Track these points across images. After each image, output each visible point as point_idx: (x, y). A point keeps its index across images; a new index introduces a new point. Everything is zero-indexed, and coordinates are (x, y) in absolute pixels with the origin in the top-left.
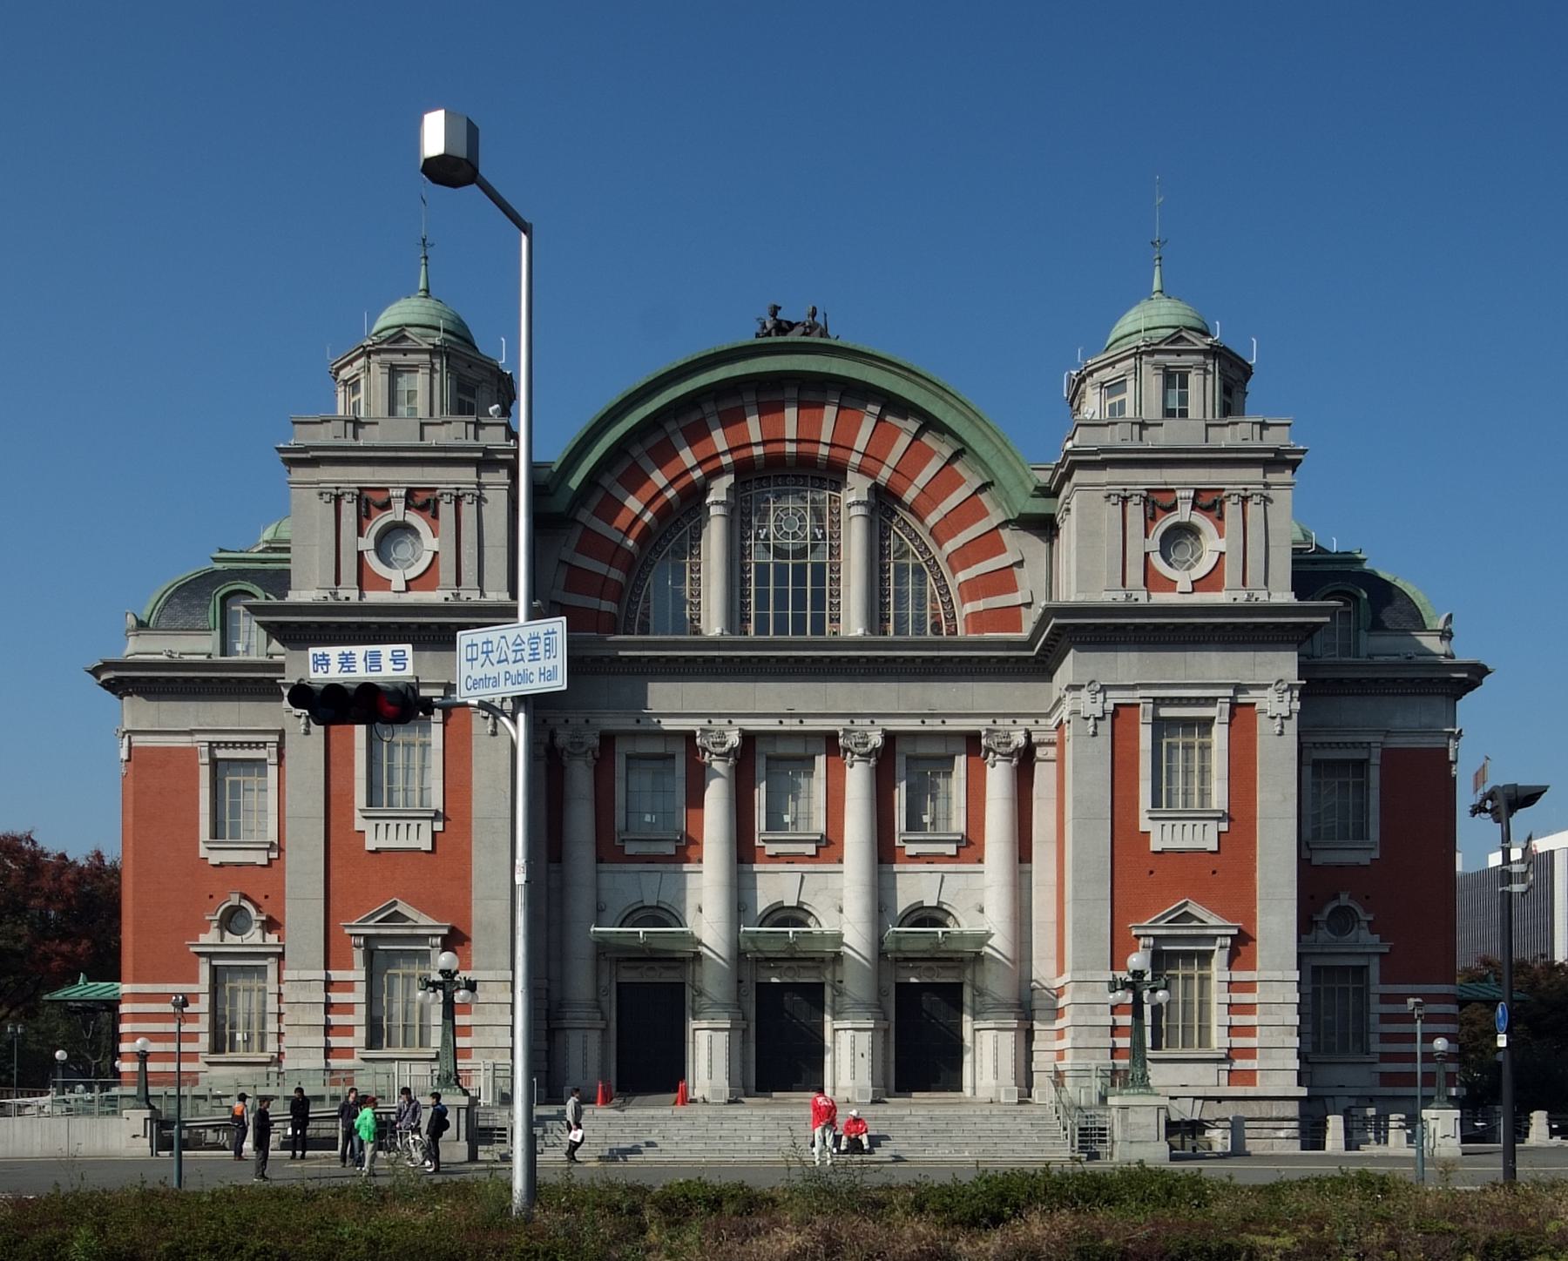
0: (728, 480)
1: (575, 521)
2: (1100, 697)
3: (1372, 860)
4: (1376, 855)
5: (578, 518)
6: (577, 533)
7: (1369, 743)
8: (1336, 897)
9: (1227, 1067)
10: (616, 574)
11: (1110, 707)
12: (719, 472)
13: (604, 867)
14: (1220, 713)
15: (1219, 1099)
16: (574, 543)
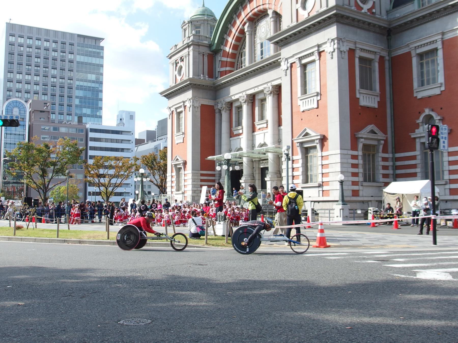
0: (247, 24)
1: (221, 49)
2: (286, 62)
3: (441, 91)
4: (443, 88)
5: (222, 48)
6: (222, 53)
7: (436, 40)
8: (424, 111)
9: (321, 189)
10: (229, 60)
11: (289, 65)
12: (245, 24)
13: (231, 139)
14: (315, 57)
15: (319, 202)
16: (221, 55)
